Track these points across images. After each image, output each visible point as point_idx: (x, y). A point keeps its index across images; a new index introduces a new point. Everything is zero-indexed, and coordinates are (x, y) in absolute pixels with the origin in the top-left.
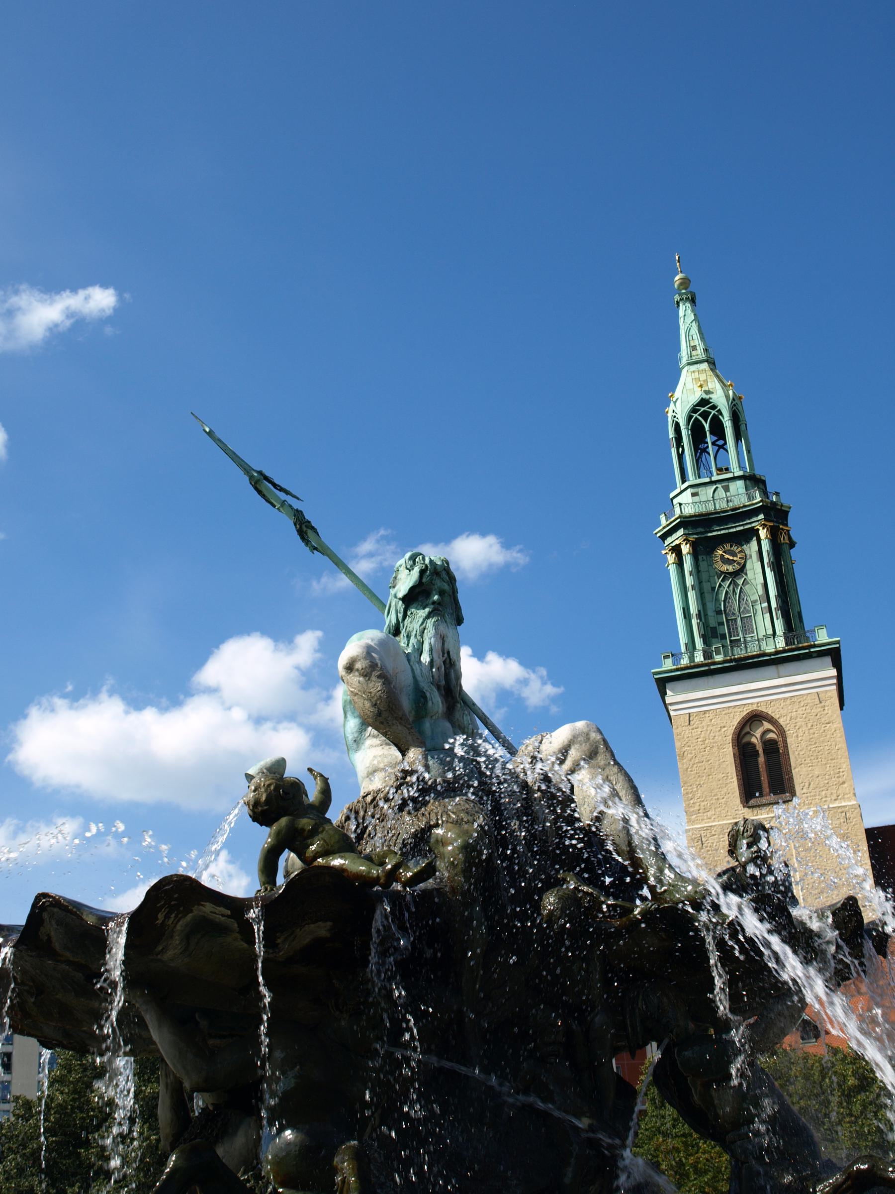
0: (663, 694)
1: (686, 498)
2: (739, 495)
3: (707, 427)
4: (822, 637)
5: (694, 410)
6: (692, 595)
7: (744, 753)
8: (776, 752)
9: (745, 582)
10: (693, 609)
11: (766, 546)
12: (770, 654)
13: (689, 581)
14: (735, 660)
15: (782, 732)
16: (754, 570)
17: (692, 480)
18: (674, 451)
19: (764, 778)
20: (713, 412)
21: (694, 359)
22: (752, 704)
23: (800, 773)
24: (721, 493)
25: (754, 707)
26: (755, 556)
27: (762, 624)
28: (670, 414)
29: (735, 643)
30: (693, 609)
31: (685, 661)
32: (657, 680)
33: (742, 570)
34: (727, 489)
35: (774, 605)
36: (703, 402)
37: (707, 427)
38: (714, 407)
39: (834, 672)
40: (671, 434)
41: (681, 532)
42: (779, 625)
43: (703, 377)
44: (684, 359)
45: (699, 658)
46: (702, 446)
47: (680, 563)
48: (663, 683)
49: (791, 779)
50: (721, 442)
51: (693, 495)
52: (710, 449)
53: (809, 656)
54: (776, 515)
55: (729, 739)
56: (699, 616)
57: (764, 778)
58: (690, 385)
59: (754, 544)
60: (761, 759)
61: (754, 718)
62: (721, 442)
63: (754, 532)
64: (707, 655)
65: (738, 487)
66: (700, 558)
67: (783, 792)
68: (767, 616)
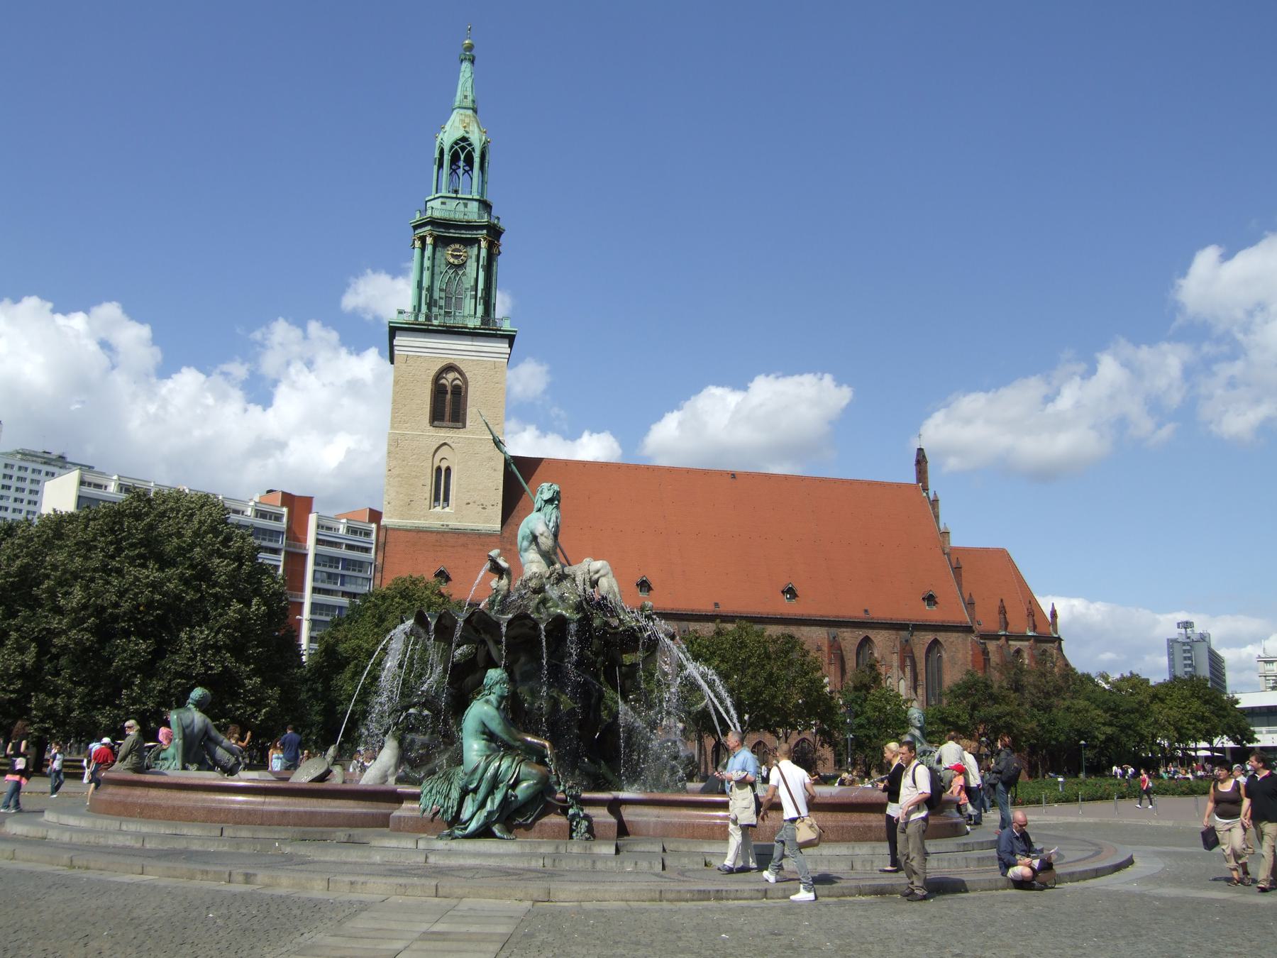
0: (392, 336)
1: (436, 204)
2: (472, 212)
4: (506, 326)
5: (456, 143)
6: (426, 274)
7: (439, 391)
8: (459, 394)
9: (464, 274)
10: (426, 283)
11: (484, 253)
13: (427, 263)
15: (466, 382)
16: (471, 267)
17: (444, 193)
18: (436, 167)
19: (448, 410)
21: (464, 105)
23: (471, 411)
24: (461, 207)
26: (474, 258)
27: (468, 305)
28: (439, 140)
30: (426, 283)
31: (412, 319)
33: (462, 266)
34: (466, 205)
35: (479, 295)
36: (464, 139)
38: (470, 145)
40: (437, 155)
41: (429, 228)
42: (480, 309)
43: (467, 120)
44: (457, 104)
45: (422, 319)
47: (423, 249)
49: (465, 414)
51: (443, 203)
52: (461, 171)
54: (495, 233)
56: (428, 290)
57: (448, 410)
58: (457, 124)
60: (449, 396)
61: (450, 368)
63: (477, 241)
64: (428, 318)
65: (474, 206)
67: (458, 421)
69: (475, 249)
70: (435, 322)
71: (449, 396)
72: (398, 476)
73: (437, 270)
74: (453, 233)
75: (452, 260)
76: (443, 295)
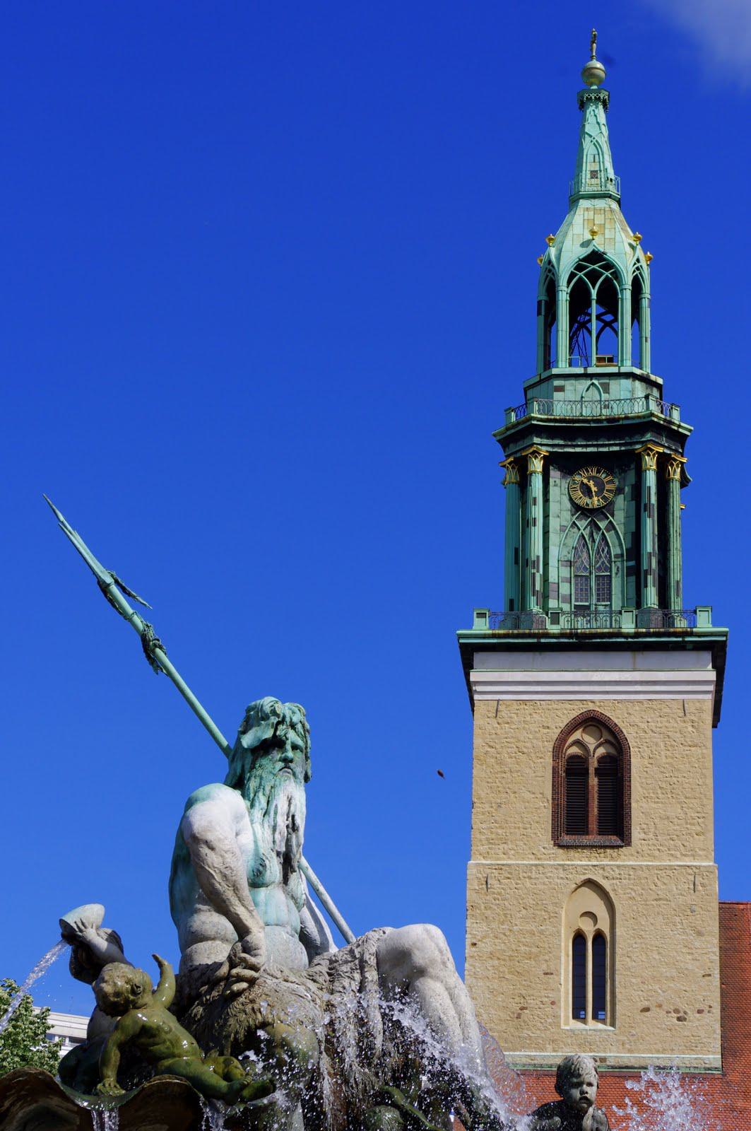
0: (468, 666)
3: (594, 293)
4: (704, 623)
5: (579, 267)
7: (572, 772)
9: (611, 527)
11: (651, 479)
12: (626, 636)
14: (577, 635)
20: (608, 274)
22: (593, 702)
25: (591, 707)
29: (581, 611)
32: (463, 646)
37: (594, 293)
38: (609, 266)
39: (712, 676)
42: (651, 596)
43: (599, 219)
46: (581, 318)
48: (469, 653)
50: (609, 318)
52: (594, 325)
53: (681, 647)
55: (550, 746)
59: (631, 477)
60: (594, 781)
61: (593, 722)
62: (609, 318)
66: (551, 481)
68: (633, 579)
69: (631, 477)
70: (554, 629)
71: (594, 781)
72: (492, 956)
73: (554, 524)
74: (579, 448)
75: (584, 501)
76: (565, 572)
